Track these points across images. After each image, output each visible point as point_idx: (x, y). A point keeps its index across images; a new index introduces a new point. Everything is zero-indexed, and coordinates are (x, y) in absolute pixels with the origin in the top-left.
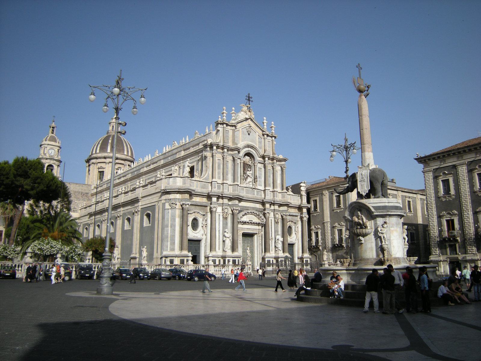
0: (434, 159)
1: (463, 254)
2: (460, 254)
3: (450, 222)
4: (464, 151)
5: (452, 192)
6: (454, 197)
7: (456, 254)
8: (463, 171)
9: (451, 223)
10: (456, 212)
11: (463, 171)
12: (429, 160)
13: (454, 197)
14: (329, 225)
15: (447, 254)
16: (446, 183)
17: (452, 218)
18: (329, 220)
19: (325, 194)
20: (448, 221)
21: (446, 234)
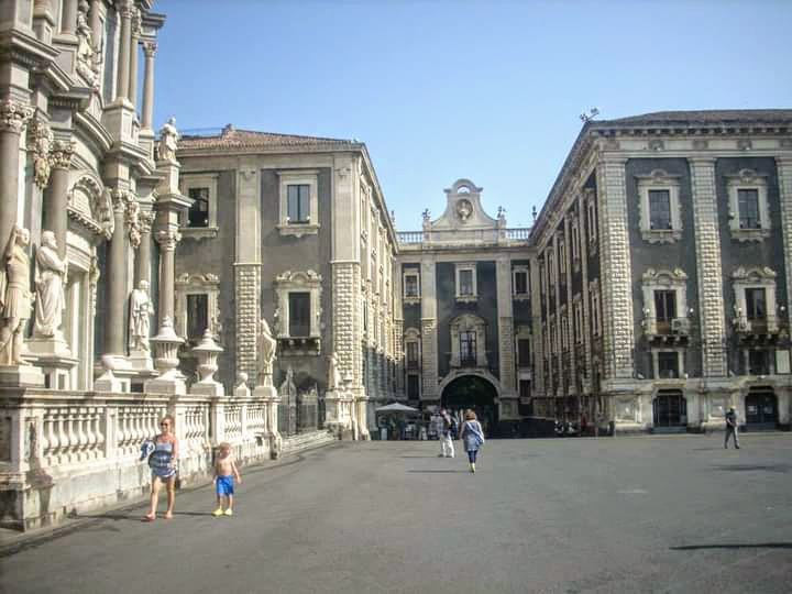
0: (638, 132)
1: (695, 376)
2: (687, 376)
3: (665, 296)
4: (718, 131)
5: (676, 224)
6: (678, 237)
7: (676, 375)
8: (703, 177)
9: (666, 303)
10: (683, 274)
11: (703, 177)
12: (625, 132)
13: (678, 237)
14: (257, 276)
15: (652, 377)
16: (658, 196)
17: (672, 288)
18: (257, 259)
19: (248, 173)
20: (658, 295)
21: (653, 330)
